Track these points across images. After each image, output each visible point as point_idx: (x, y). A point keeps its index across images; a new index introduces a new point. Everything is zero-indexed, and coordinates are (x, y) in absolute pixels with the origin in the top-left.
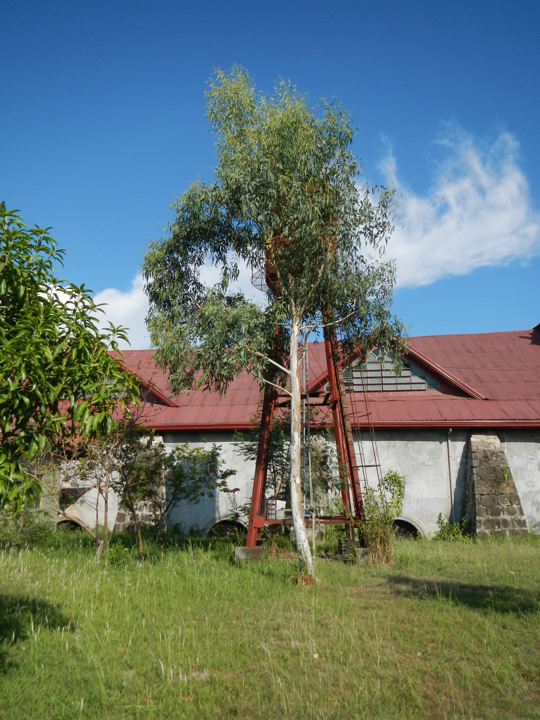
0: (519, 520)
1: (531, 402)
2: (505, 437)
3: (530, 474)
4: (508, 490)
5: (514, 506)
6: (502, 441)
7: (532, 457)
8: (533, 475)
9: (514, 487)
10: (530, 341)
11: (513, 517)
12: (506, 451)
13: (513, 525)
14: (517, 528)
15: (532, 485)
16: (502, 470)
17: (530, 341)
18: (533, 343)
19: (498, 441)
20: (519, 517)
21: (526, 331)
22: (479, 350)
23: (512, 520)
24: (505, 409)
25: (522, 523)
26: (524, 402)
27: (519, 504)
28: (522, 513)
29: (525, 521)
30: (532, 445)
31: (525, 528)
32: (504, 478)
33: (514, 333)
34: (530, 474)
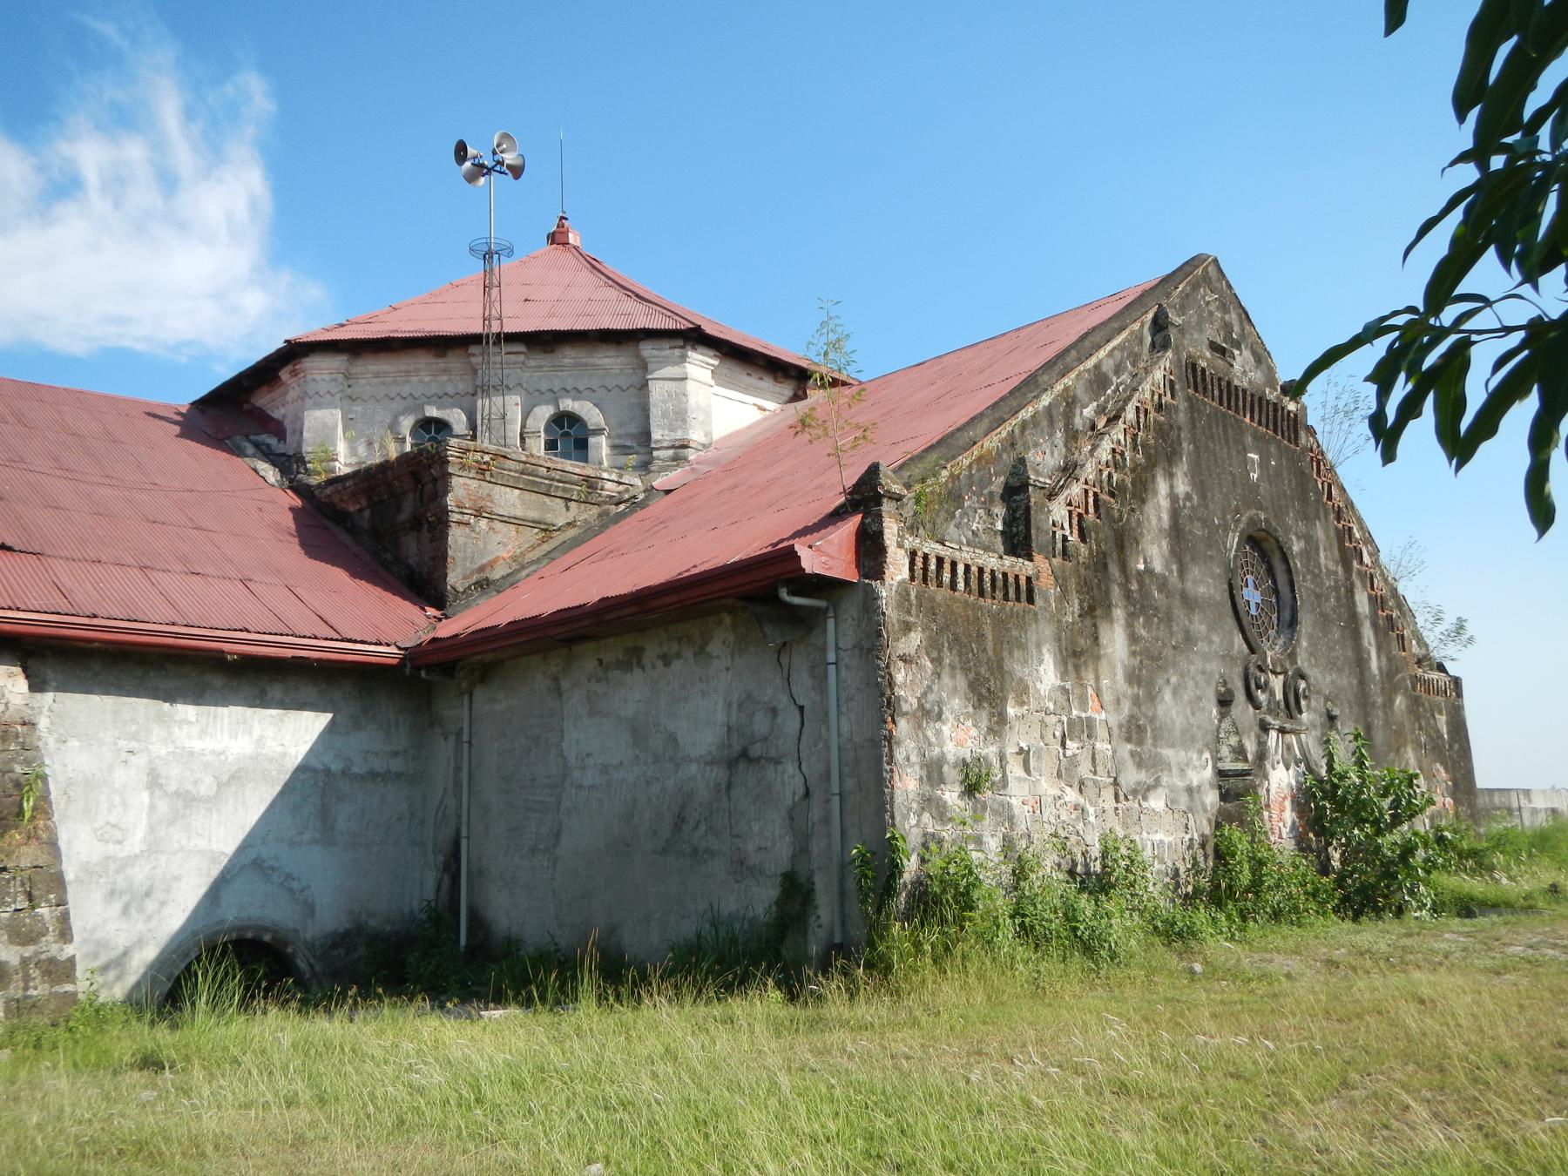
0: (52, 961)
1: (154, 575)
2: (50, 673)
3: (117, 799)
4: (28, 856)
5: (43, 910)
6: (36, 686)
7: (134, 745)
8: (124, 804)
9: (53, 845)
10: (177, 429)
11: (28, 951)
12: (43, 723)
13: (27, 979)
14: (39, 990)
15: (118, 834)
16: (18, 785)
17: (177, 429)
18: (181, 436)
19: (21, 684)
20: (55, 947)
21: (165, 406)
22: (10, 419)
23: (25, 962)
24: (67, 582)
25: (61, 970)
26: (136, 574)
27: (61, 902)
28: (65, 934)
29: (72, 960)
30: (140, 708)
31: (69, 987)
32: (21, 813)
33: (135, 403)
34: (117, 799)
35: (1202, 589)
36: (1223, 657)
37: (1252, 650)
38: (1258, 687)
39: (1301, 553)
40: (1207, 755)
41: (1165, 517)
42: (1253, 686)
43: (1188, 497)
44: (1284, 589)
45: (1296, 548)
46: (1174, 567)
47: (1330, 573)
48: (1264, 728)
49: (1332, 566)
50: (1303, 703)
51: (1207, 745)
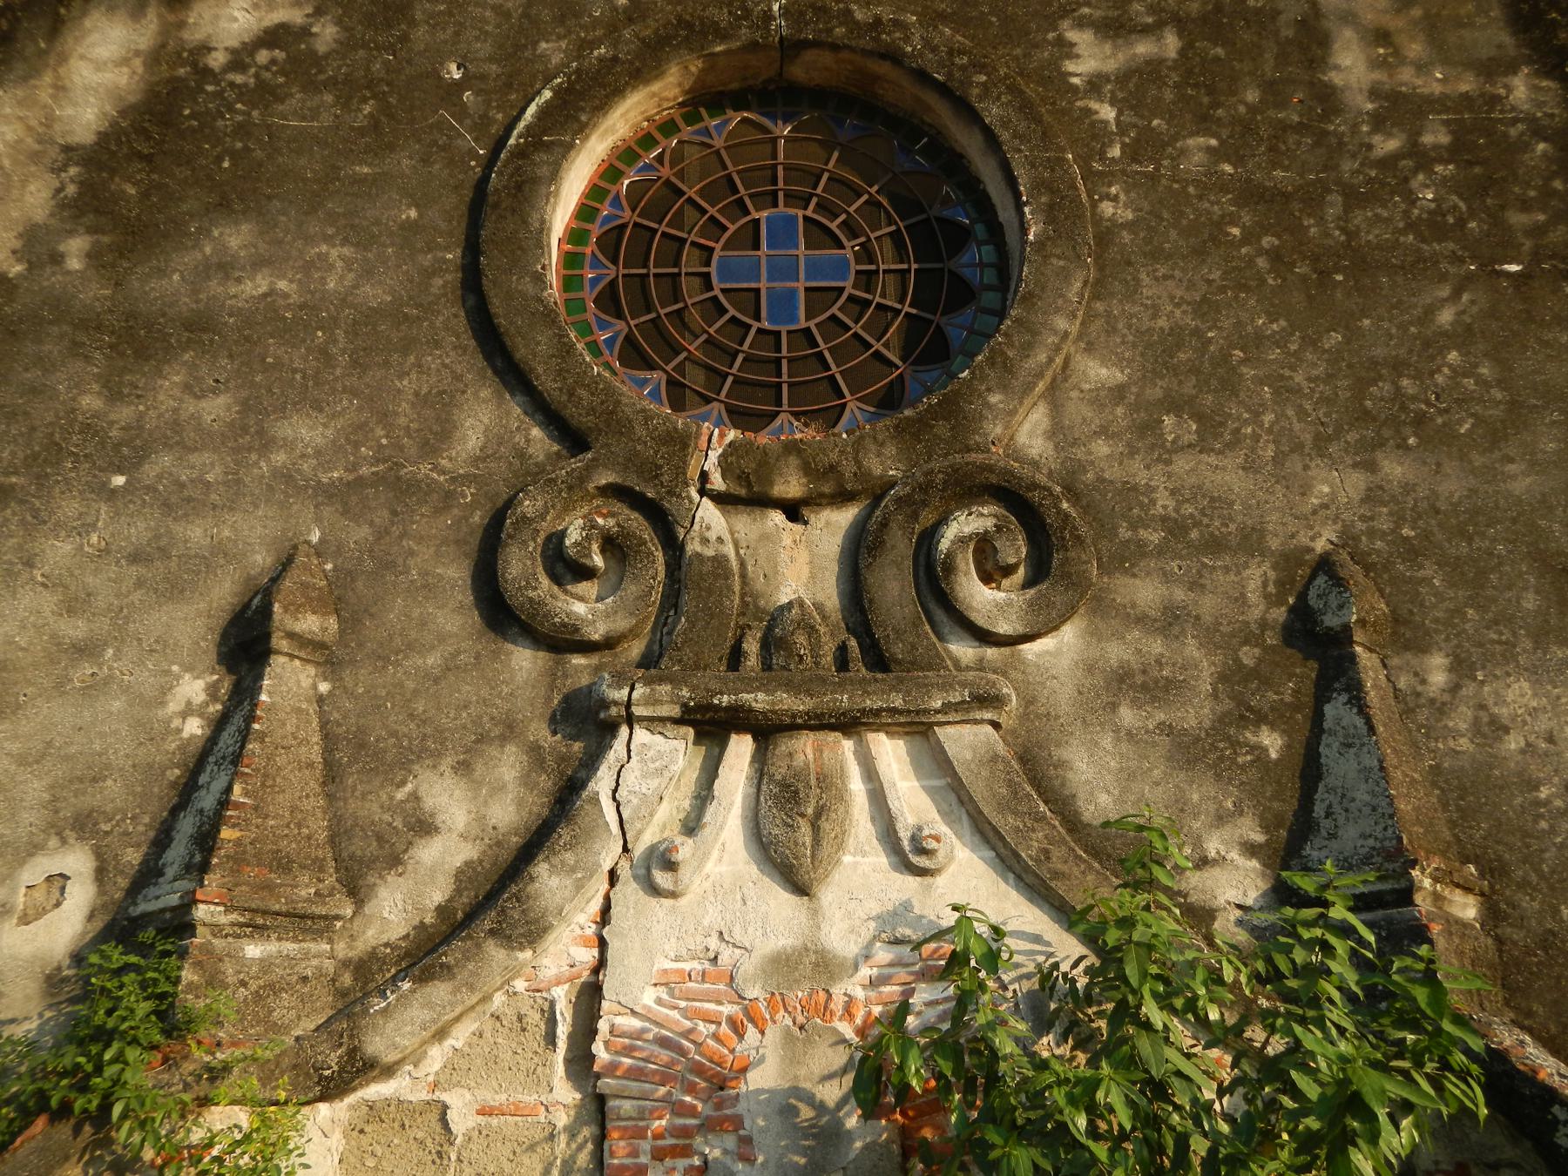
35: (256, 285)
36: (329, 493)
37: (573, 439)
38: (566, 568)
39: (1133, 87)
40: (77, 862)
41: (85, 117)
42: (521, 566)
43: (273, 37)
44: (1006, 214)
45: (1089, 57)
46: (75, 251)
47: (1397, 108)
48: (590, 724)
49: (1435, 83)
50: (982, 598)
51: (83, 826)
